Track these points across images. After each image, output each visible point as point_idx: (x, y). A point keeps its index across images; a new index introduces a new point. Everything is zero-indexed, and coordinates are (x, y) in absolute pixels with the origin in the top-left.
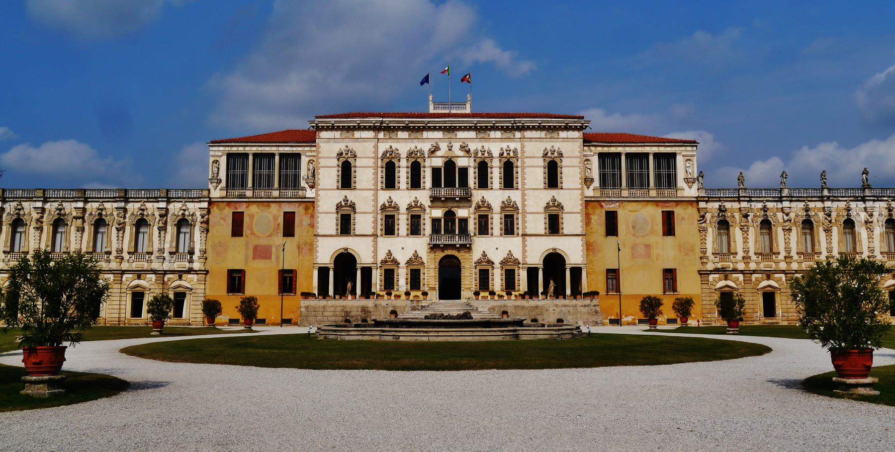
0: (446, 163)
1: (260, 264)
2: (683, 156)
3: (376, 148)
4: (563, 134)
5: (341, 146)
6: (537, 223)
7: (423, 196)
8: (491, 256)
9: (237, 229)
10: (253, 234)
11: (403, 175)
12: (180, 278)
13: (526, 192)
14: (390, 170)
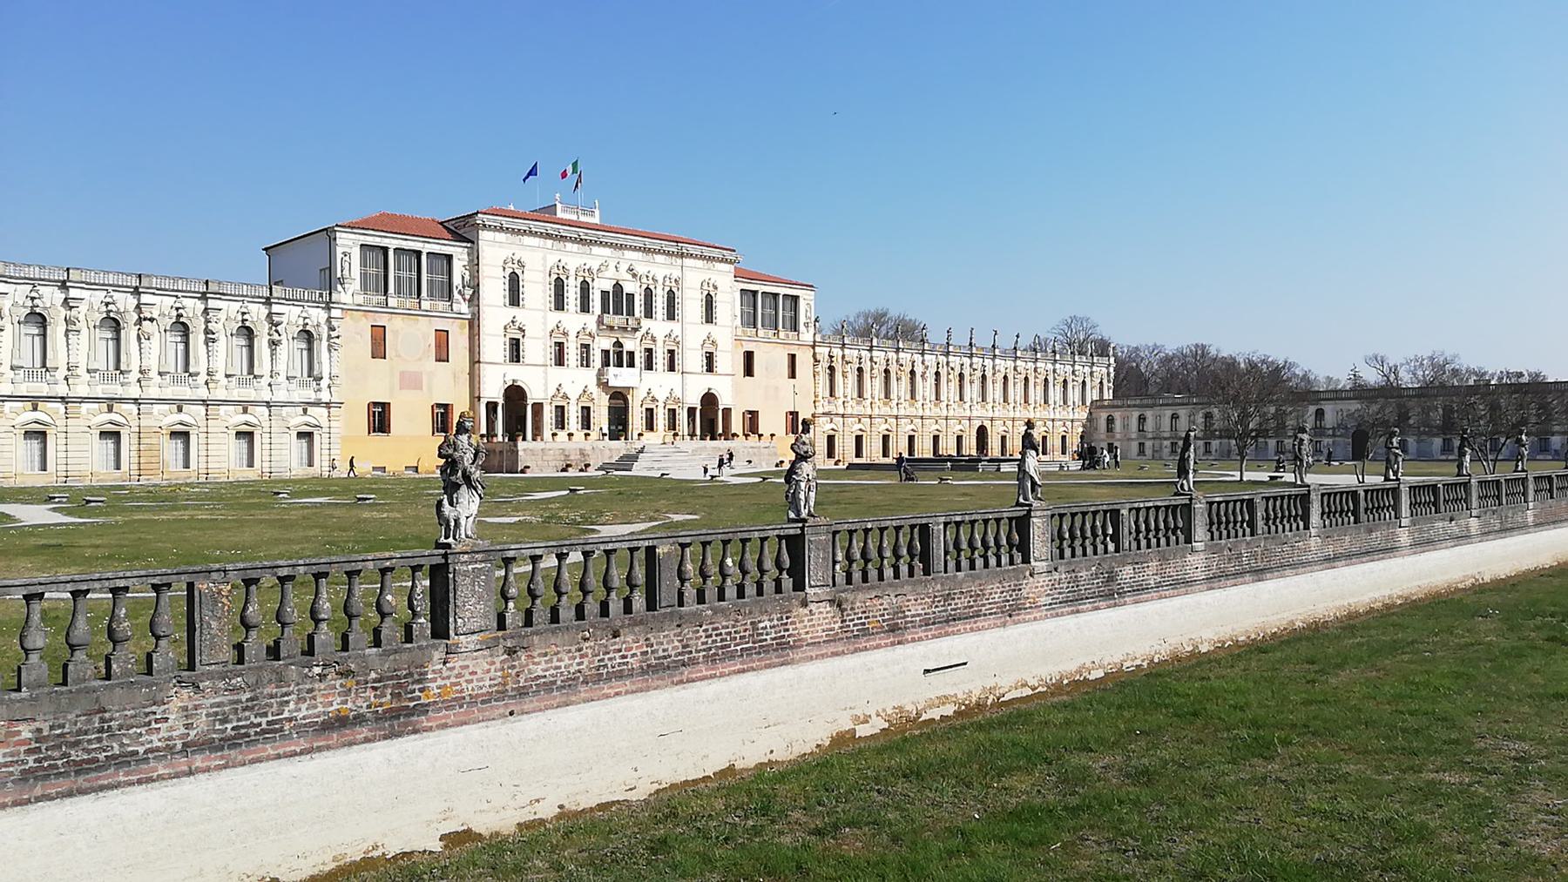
3: (544, 259)
5: (505, 253)
6: (692, 359)
8: (654, 393)
9: (379, 350)
10: (399, 356)
14: (559, 286)
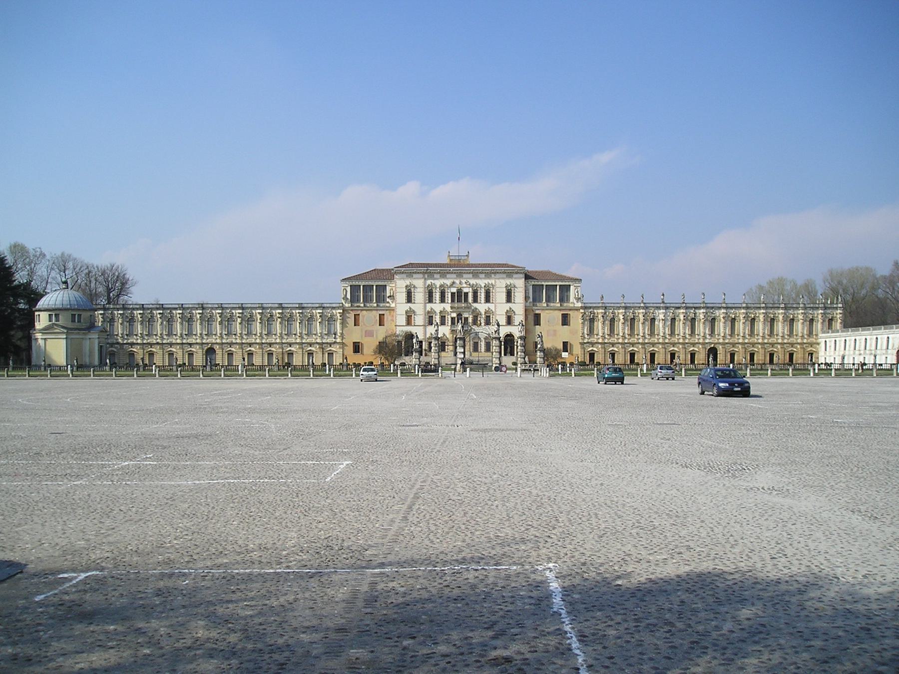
0: (457, 290)
4: (515, 276)
5: (408, 282)
6: (503, 321)
7: (447, 307)
10: (364, 324)
11: (437, 296)
12: (330, 346)
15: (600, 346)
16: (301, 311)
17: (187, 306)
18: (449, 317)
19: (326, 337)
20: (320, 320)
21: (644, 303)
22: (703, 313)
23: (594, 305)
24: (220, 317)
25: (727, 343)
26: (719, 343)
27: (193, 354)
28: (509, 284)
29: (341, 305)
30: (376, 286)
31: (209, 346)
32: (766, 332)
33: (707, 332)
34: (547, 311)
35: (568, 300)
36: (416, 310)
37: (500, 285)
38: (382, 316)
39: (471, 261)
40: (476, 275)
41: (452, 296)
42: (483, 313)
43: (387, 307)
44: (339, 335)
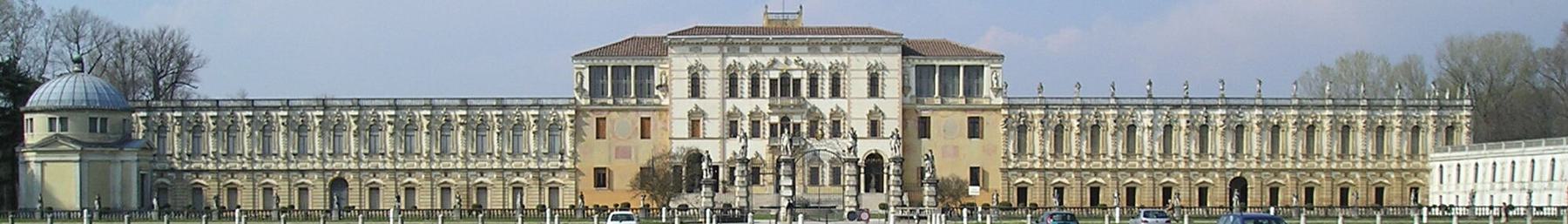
0: (781, 75)
1: (622, 162)
2: (992, 68)
4: (884, 49)
5: (692, 60)
6: (862, 129)
7: (763, 104)
9: (600, 134)
10: (614, 136)
11: (745, 85)
12: (554, 175)
13: (852, 101)
15: (1036, 175)
16: (500, 112)
17: (297, 103)
18: (766, 122)
19: (546, 159)
20: (534, 129)
21: (1116, 98)
22: (1222, 115)
23: (1027, 102)
24: (355, 122)
25: (1264, 170)
26: (1251, 170)
27: (307, 189)
28: (874, 63)
29: (573, 101)
30: (636, 67)
31: (336, 176)
32: (1335, 150)
33: (1229, 149)
34: (942, 113)
35: (979, 93)
36: (706, 111)
37: (857, 65)
38: (646, 122)
39: (807, 21)
40: (814, 48)
41: (771, 84)
42: (828, 116)
43: (655, 105)
44: (569, 154)
